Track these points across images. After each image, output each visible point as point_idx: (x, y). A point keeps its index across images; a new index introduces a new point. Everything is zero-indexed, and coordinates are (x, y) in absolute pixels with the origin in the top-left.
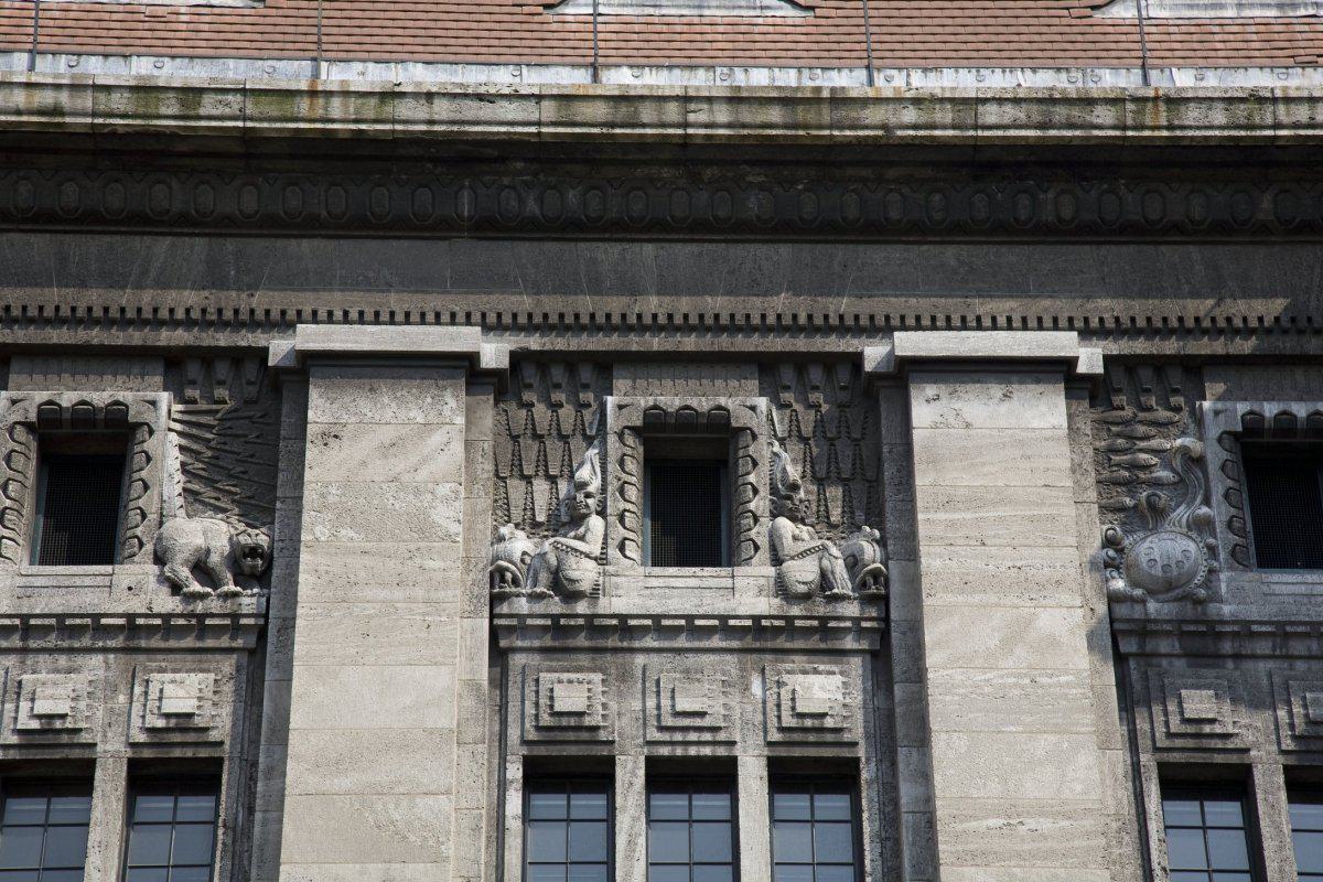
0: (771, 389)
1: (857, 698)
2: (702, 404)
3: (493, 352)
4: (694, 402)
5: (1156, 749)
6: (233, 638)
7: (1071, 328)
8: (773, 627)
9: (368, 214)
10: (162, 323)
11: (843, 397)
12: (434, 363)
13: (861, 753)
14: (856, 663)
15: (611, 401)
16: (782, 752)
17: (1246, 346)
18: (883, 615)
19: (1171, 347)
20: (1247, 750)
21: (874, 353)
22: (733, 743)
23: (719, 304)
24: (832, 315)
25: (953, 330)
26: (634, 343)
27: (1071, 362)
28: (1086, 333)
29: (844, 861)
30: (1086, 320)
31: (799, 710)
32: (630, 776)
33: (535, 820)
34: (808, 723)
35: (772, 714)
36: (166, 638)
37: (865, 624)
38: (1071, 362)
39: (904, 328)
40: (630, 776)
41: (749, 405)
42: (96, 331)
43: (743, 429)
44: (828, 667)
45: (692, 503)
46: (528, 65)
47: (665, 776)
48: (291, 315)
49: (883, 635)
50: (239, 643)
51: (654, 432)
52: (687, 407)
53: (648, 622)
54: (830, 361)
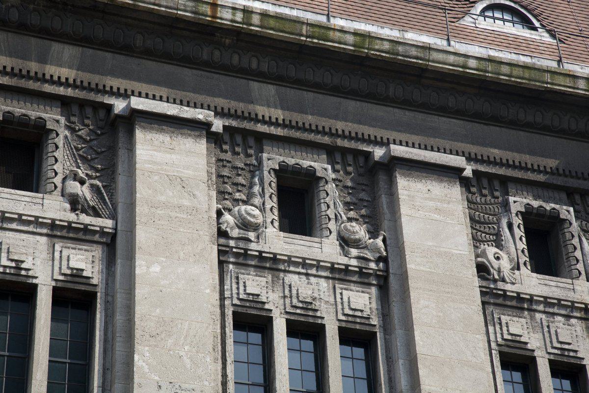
0: (332, 161)
1: (374, 305)
2: (306, 163)
3: (218, 125)
4: (301, 162)
5: (498, 345)
6: (68, 232)
7: (463, 155)
8: (339, 269)
9: (92, 37)
10: (46, 81)
11: (362, 170)
12: (181, 123)
13: (377, 330)
14: (374, 290)
15: (265, 155)
16: (344, 325)
17: (541, 178)
18: (385, 270)
19: (501, 171)
20: (533, 351)
21: (379, 153)
22: (323, 318)
23: (310, 119)
24: (371, 135)
25: (446, 154)
26: (273, 130)
27: (462, 170)
28: (469, 159)
29: (258, 362)
30: (470, 154)
31: (247, 292)
32: (280, 327)
33: (352, 355)
34: (251, 298)
35: (340, 307)
36: (85, 234)
37: (378, 273)
38: (462, 170)
39: (395, 143)
40: (280, 327)
41: (320, 166)
42: (319, 136)
43: (321, 178)
44: (358, 289)
45: (298, 207)
46: (297, 9)
47: (295, 330)
48: (129, 92)
49: (386, 278)
50: (104, 240)
51: (528, 215)
52: (311, 166)
53: (542, 299)
54: (357, 153)
